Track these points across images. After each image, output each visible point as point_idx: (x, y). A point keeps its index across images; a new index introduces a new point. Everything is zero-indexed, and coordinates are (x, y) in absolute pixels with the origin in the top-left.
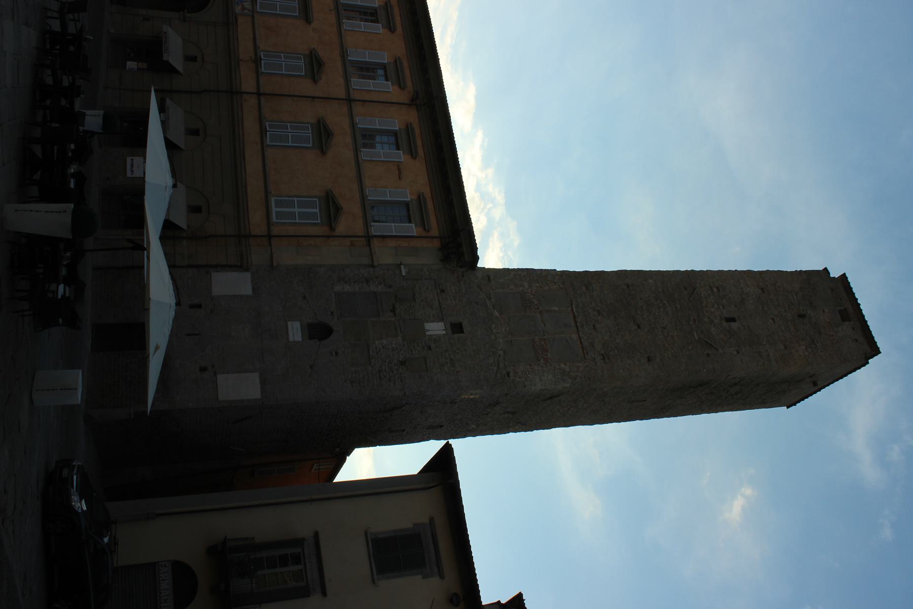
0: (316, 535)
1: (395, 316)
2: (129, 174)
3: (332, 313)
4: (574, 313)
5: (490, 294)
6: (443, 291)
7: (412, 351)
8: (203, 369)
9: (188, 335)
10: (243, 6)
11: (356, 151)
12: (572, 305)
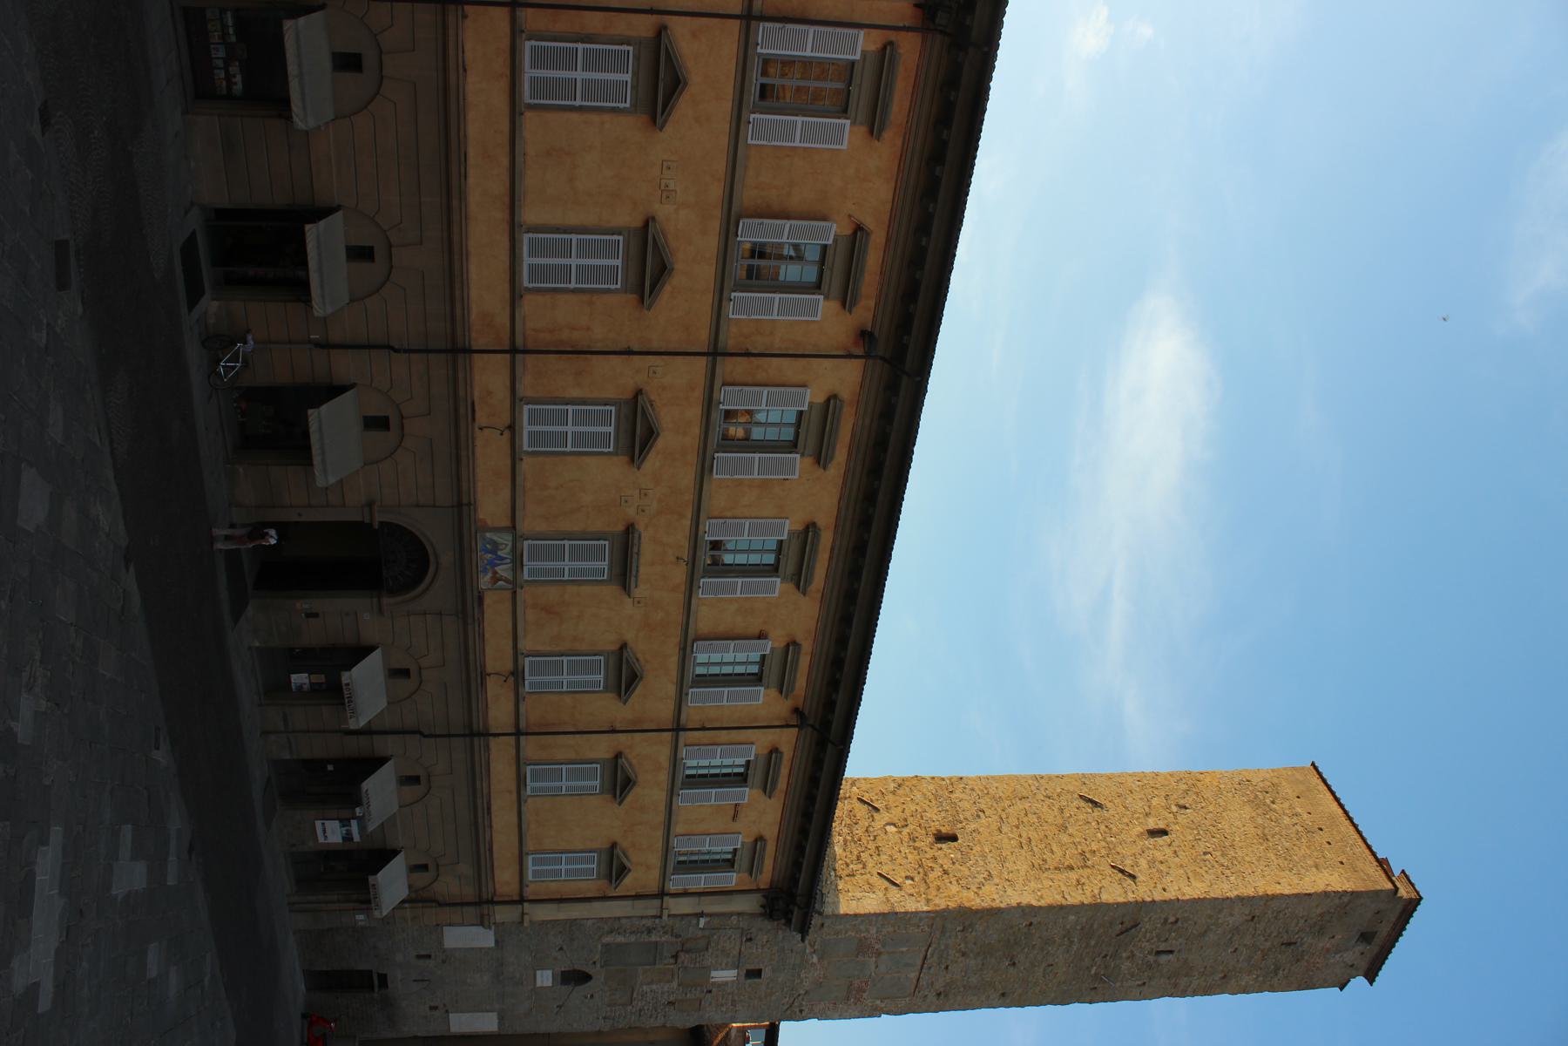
2: (321, 839)
3: (594, 963)
5: (815, 942)
6: (750, 939)
7: (686, 994)
9: (415, 981)
10: (495, 573)
11: (672, 793)
12: (930, 946)
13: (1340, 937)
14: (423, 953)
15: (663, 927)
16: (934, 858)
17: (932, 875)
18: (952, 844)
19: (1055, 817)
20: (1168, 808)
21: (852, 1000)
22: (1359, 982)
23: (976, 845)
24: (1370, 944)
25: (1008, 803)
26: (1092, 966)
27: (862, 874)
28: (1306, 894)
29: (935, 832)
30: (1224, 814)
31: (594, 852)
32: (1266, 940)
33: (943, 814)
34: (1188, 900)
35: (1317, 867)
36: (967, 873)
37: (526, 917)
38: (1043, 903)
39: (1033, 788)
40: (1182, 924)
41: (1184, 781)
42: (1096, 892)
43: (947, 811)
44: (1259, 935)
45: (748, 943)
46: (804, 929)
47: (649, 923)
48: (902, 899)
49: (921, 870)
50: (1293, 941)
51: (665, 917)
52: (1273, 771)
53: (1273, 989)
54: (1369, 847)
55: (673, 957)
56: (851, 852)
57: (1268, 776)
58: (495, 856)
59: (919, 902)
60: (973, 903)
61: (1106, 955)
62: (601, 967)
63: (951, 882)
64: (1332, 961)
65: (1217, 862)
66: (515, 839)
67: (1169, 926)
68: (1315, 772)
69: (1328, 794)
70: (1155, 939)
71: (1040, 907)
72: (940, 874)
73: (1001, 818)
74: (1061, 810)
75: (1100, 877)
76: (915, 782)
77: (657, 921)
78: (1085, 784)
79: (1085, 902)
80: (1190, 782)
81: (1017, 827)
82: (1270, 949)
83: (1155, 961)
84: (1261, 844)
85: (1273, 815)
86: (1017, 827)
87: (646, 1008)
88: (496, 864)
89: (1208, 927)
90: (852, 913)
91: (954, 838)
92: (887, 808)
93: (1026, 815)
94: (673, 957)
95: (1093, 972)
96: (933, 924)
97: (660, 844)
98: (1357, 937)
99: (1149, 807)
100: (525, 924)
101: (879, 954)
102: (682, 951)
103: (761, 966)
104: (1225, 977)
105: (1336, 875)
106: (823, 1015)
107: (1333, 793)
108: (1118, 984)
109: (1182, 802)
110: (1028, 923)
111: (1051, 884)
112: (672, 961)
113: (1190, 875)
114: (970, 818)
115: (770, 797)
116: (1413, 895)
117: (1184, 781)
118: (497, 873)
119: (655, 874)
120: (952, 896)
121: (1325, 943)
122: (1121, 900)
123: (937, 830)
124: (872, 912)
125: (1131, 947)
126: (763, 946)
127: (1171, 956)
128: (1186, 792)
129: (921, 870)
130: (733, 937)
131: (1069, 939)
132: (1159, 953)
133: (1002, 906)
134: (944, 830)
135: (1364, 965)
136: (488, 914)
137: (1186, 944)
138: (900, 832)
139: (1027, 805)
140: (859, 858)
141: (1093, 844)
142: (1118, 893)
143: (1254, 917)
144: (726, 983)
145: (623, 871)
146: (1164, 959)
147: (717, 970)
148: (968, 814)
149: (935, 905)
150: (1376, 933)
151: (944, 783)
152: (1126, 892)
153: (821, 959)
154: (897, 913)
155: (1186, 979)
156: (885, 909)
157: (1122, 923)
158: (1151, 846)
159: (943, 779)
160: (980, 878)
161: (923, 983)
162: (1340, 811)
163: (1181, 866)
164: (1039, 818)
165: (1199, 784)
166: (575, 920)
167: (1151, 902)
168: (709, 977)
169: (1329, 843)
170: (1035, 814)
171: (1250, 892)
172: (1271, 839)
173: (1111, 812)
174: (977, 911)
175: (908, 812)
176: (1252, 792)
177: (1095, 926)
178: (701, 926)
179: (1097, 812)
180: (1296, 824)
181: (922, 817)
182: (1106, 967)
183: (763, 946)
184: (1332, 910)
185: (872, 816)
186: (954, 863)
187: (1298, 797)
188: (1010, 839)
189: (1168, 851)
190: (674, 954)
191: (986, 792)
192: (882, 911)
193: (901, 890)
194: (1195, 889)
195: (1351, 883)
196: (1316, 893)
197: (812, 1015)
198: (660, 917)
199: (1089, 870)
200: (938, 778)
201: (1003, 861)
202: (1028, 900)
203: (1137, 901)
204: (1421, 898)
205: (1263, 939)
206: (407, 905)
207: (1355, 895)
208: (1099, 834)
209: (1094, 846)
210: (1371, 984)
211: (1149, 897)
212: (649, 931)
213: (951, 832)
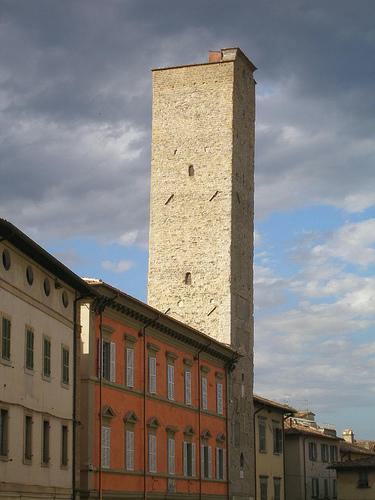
179: (176, 199)
204: (238, 49)
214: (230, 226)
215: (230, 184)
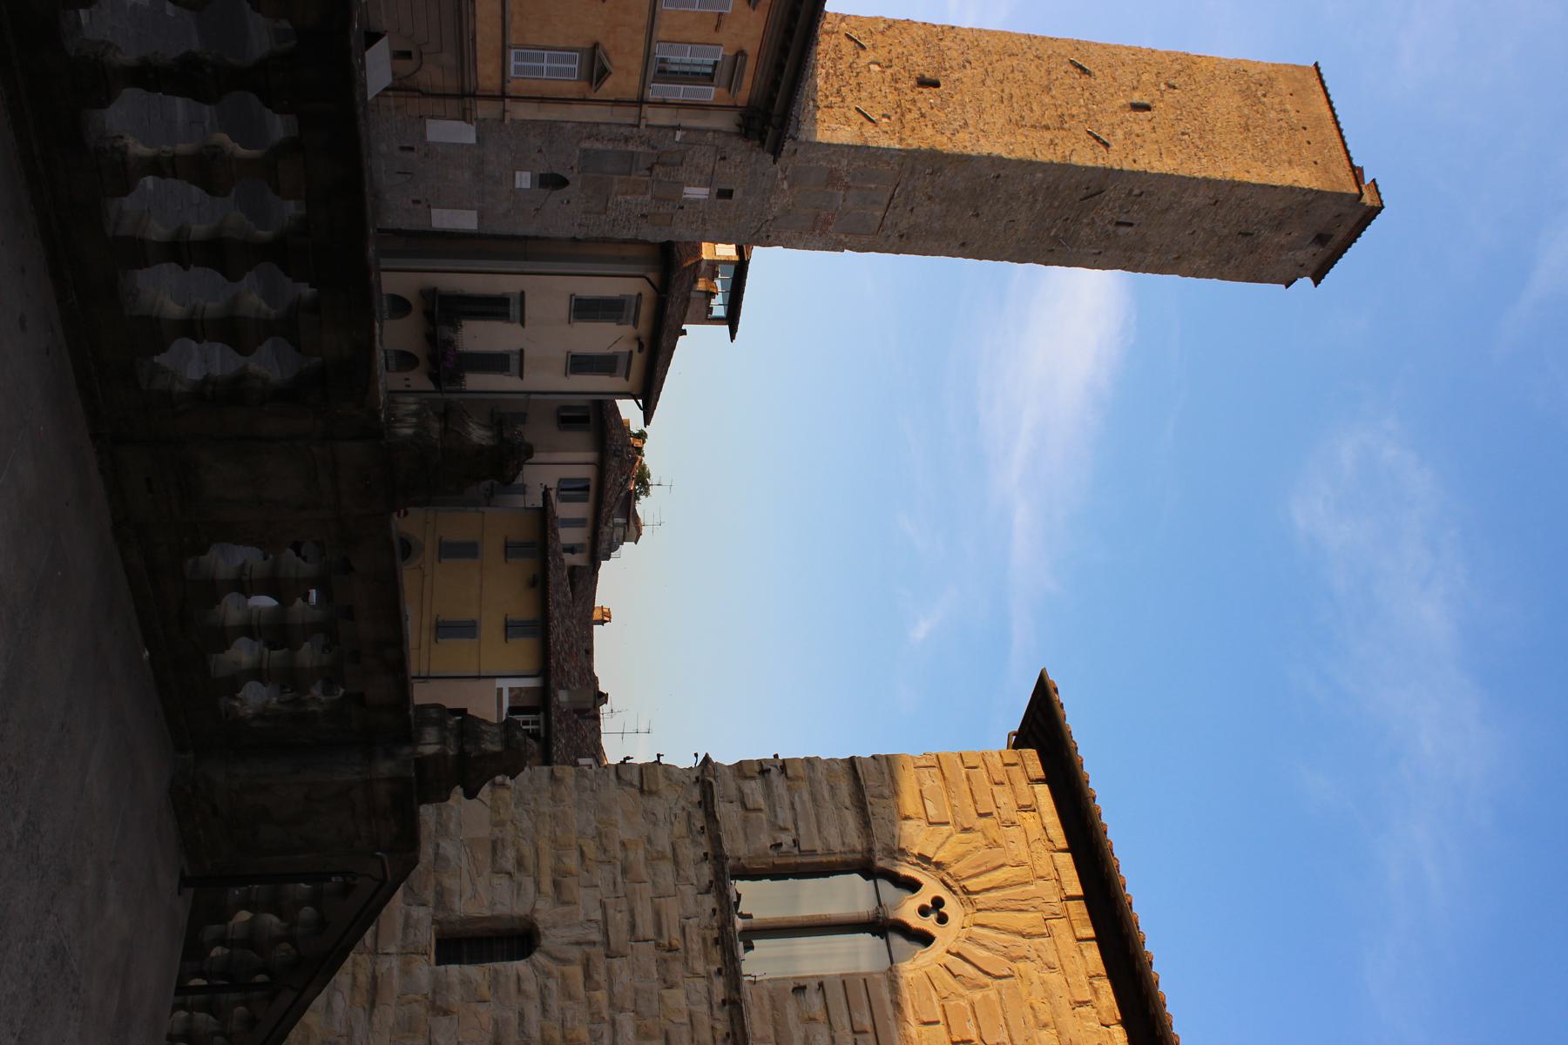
0: (523, 294)
1: (650, 176)
3: (572, 168)
4: (894, 194)
5: (786, 168)
6: (724, 158)
7: (659, 208)
8: (416, 202)
9: (399, 173)
12: (897, 186)
13: (1296, 234)
14: (407, 145)
15: (640, 137)
16: (914, 101)
17: (909, 117)
18: (933, 90)
19: (1041, 77)
20: (1157, 85)
21: (818, 231)
22: (1305, 283)
23: (956, 94)
24: (1323, 246)
25: (998, 57)
26: (1052, 227)
27: (840, 107)
28: (1272, 186)
29: (918, 76)
30: (1212, 99)
31: (576, 51)
32: (1224, 227)
33: (929, 60)
34: (1155, 174)
35: (1290, 162)
36: (944, 119)
37: (508, 116)
38: (1013, 156)
39: (1025, 46)
40: (1146, 197)
41: (1179, 61)
42: (1067, 153)
43: (933, 57)
44: (1218, 221)
45: (722, 162)
46: (776, 152)
47: (626, 131)
48: (875, 135)
49: (899, 110)
50: (1250, 232)
51: (642, 126)
52: (1273, 65)
53: (1222, 277)
54: (1347, 152)
55: (648, 169)
56: (832, 85)
57: (1266, 69)
58: (478, 46)
59: (892, 139)
60: (944, 147)
61: (1067, 219)
62: (579, 172)
63: (926, 126)
64: (1284, 258)
65: (1193, 143)
66: (498, 32)
67: (1132, 198)
68: (1315, 73)
69: (1323, 97)
70: (1117, 210)
71: (1010, 160)
72: (917, 116)
73: (987, 72)
74: (1049, 72)
75: (1074, 140)
76: (905, 25)
77: (635, 129)
78: (1078, 49)
79: (1055, 161)
80: (1186, 63)
81: (1002, 82)
82: (1226, 237)
83: (1114, 232)
84: (1241, 133)
85: (1261, 108)
86: (1002, 82)
87: (620, 218)
88: (479, 55)
89: (1171, 204)
90: (826, 142)
91: (936, 85)
92: (874, 47)
93: (1013, 71)
94: (648, 169)
95: (1052, 234)
96: (902, 164)
97: (641, 50)
98: (1310, 240)
99: (1138, 81)
100: (506, 122)
101: (848, 188)
102: (657, 163)
103: (734, 188)
104: (1178, 258)
105: (1307, 173)
106: (788, 244)
107: (1327, 96)
108: (1075, 250)
109: (1172, 82)
110: (996, 175)
111: (1024, 139)
112: (648, 173)
113: (1163, 151)
114: (956, 67)
115: (754, 9)
116: (1376, 204)
117: (1179, 61)
118: (480, 65)
119: (635, 81)
120: (925, 138)
121: (1281, 238)
122: (1090, 164)
123: (920, 74)
124: (845, 143)
125: (1092, 214)
126: (736, 166)
127: (1129, 229)
128: (1179, 72)
129: (899, 110)
130: (708, 154)
131: (1033, 197)
132: (1119, 224)
133: (974, 153)
134: (927, 75)
135: (1313, 266)
136: (471, 110)
137: (1147, 218)
138: (884, 72)
139: (1015, 63)
140: (839, 91)
141: (1074, 108)
142: (1089, 157)
143: (1217, 202)
144: (698, 201)
145: (604, 73)
146: (1122, 230)
147: (689, 186)
148: (954, 63)
149: (908, 144)
150: (1332, 236)
151: (935, 30)
152: (1096, 158)
153: (791, 186)
154: (869, 147)
155: (1140, 254)
156: (859, 142)
157: (1087, 188)
158: (1131, 119)
159: (935, 26)
160: (956, 125)
161: (887, 222)
162: (1329, 114)
163: (1157, 141)
164: (1025, 76)
165: (1194, 66)
166: (555, 121)
167: (1119, 170)
168: (681, 192)
169: (1309, 143)
170: (1021, 71)
171: (1218, 175)
172: (1252, 131)
173: (1098, 81)
174: (947, 156)
175: (894, 54)
176: (1246, 82)
177: (1061, 187)
178: (677, 139)
179: (1084, 78)
180: (1282, 120)
181: (907, 60)
182: (1066, 231)
183: (736, 166)
184: (1294, 207)
185: (858, 53)
186: (932, 108)
187: (1291, 95)
188: (992, 93)
189: (1147, 126)
190: (649, 166)
191: (976, 43)
192: (855, 144)
193: (876, 126)
194: (1166, 166)
195: (1319, 183)
196: (1282, 186)
197: (777, 242)
198: (638, 126)
199: (1065, 133)
200: (930, 24)
201: (981, 112)
202: (999, 151)
203: (1105, 168)
204: (1383, 207)
205: (1222, 225)
206: (390, 93)
207: (1319, 194)
208: (1082, 101)
209: (1074, 111)
210: (1316, 286)
211: (1118, 165)
212: (627, 140)
213: (934, 78)
214: (1040, 158)
215: (1126, 167)
